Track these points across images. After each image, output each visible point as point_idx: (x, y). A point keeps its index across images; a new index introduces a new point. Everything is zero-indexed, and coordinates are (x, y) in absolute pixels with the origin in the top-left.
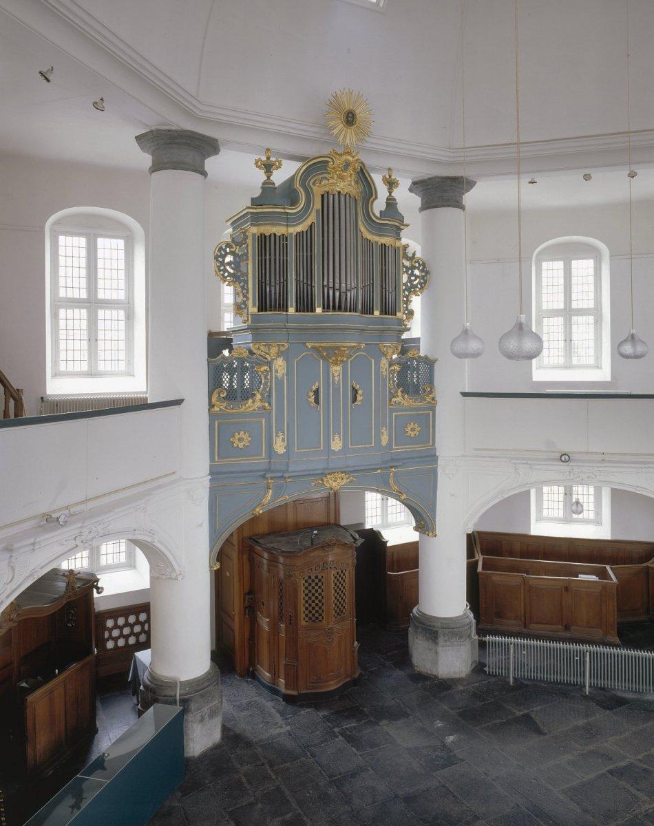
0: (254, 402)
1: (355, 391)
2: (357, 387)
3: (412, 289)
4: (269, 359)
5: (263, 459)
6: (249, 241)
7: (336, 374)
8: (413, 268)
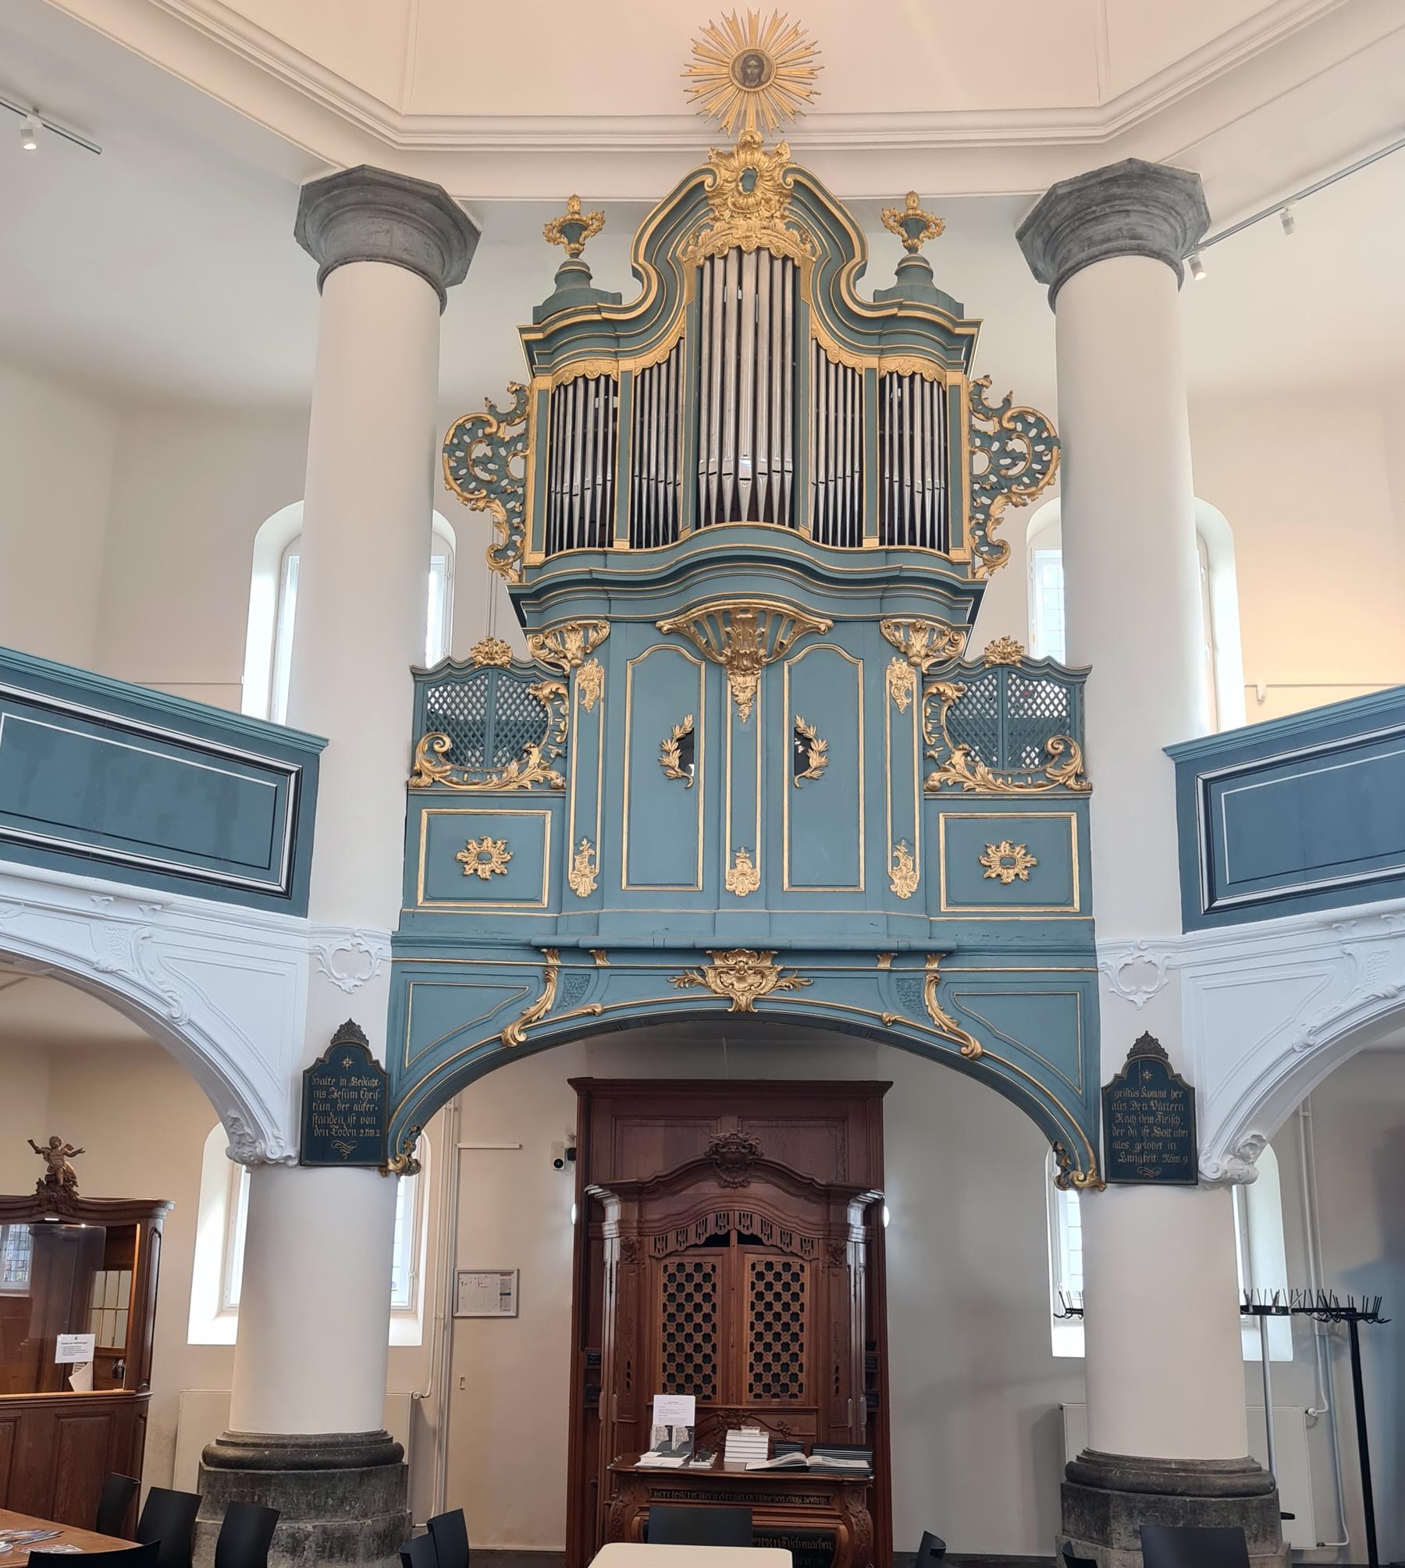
0: (521, 771)
2: (811, 733)
3: (1000, 486)
4: (567, 668)
6: (533, 408)
7: (742, 697)
8: (1006, 435)
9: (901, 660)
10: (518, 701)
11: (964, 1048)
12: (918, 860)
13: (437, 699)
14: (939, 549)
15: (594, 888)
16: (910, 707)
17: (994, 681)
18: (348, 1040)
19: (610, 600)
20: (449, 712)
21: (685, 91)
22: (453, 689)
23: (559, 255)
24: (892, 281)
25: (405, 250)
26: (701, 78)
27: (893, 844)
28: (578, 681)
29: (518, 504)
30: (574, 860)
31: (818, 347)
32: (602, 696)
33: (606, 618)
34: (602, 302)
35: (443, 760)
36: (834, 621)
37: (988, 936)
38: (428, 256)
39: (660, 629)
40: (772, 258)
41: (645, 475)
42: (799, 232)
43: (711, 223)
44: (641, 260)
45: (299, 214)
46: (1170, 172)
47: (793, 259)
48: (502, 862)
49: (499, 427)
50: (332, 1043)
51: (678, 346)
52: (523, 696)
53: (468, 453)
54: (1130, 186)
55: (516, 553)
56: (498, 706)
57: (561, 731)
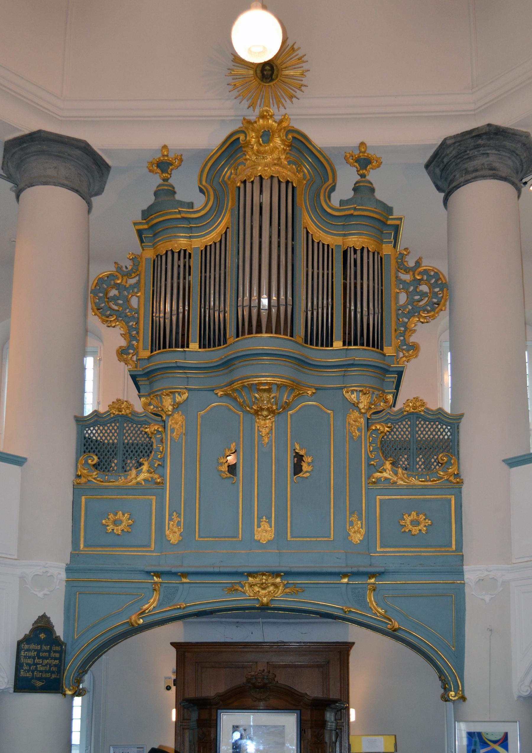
0: (137, 475)
1: (299, 458)
5: (151, 551)
9: (355, 411)
10: (136, 435)
11: (389, 625)
12: (364, 523)
13: (93, 433)
14: (378, 348)
15: (180, 539)
16: (360, 437)
17: (409, 423)
19: (188, 377)
20: (99, 438)
21: (228, 85)
22: (99, 428)
23: (156, 180)
24: (351, 194)
25: (67, 178)
26: (238, 77)
28: (170, 423)
29: (134, 323)
30: (169, 524)
31: (308, 232)
32: (184, 432)
33: (186, 388)
34: (181, 208)
35: (93, 469)
36: (316, 389)
37: (403, 564)
38: (80, 181)
39: (217, 394)
40: (280, 182)
41: (207, 307)
42: (296, 166)
43: (244, 162)
44: (204, 183)
45: (4, 157)
47: (292, 183)
48: (128, 525)
49: (122, 280)
50: (33, 625)
51: (226, 233)
52: (139, 432)
53: (106, 294)
55: (134, 352)
56: (124, 438)
57: (161, 452)
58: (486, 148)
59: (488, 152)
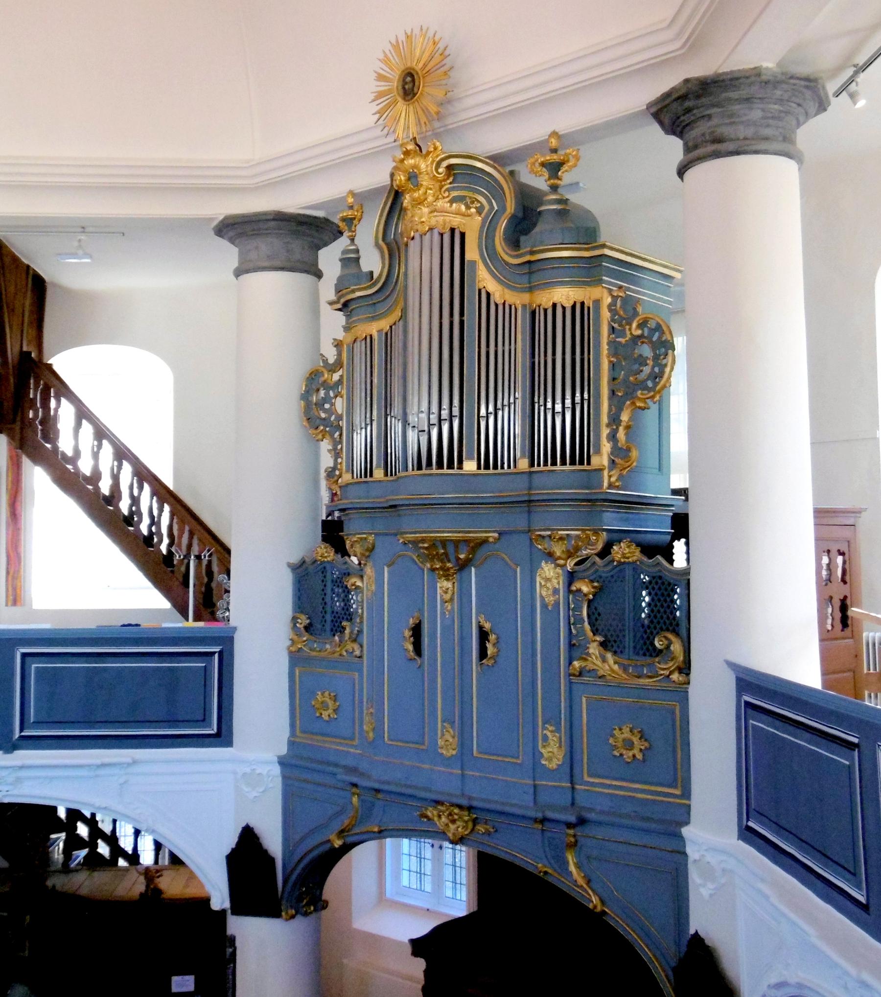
2: (487, 626)
18: (248, 836)
27: (544, 723)
31: (488, 295)
46: (729, 76)
54: (698, 97)
58: (701, 109)
59: (708, 112)
